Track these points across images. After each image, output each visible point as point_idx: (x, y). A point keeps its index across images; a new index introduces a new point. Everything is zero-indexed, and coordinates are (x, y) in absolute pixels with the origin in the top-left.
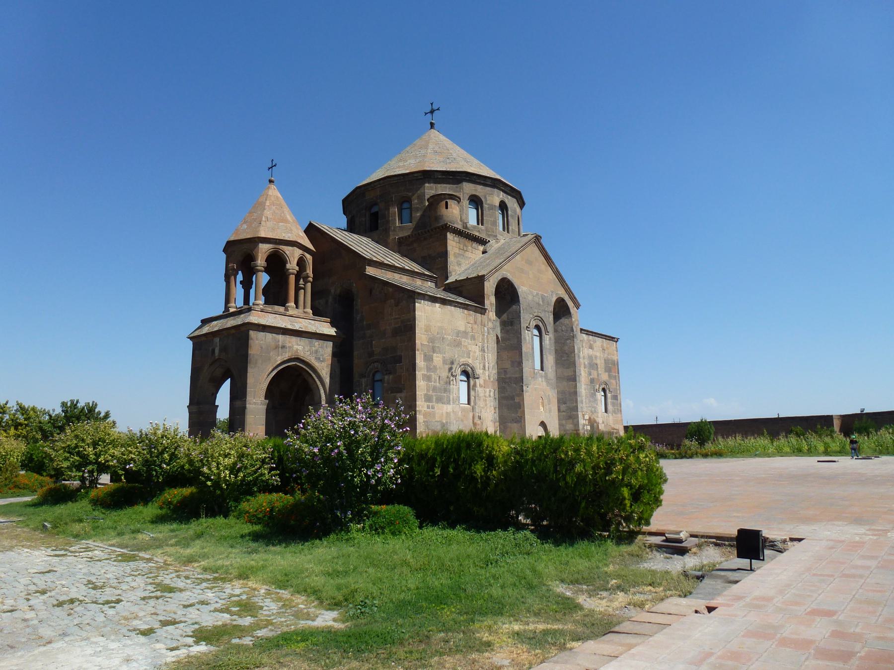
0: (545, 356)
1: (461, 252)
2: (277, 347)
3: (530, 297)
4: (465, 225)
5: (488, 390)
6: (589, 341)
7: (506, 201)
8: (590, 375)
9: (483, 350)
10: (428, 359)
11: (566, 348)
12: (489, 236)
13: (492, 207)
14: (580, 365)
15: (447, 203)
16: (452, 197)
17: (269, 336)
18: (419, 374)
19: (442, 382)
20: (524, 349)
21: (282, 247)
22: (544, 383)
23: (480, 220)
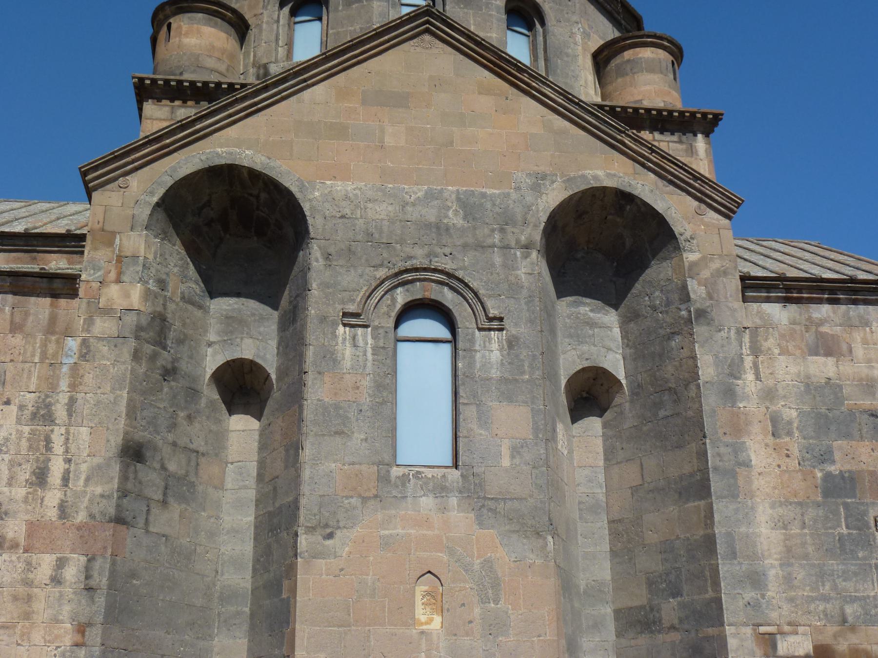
0: (468, 412)
3: (382, 211)
5: (46, 563)
6: (811, 323)
8: (825, 457)
9: (43, 415)
11: (669, 369)
14: (738, 426)
15: (169, 26)
20: (318, 392)
22: (459, 518)
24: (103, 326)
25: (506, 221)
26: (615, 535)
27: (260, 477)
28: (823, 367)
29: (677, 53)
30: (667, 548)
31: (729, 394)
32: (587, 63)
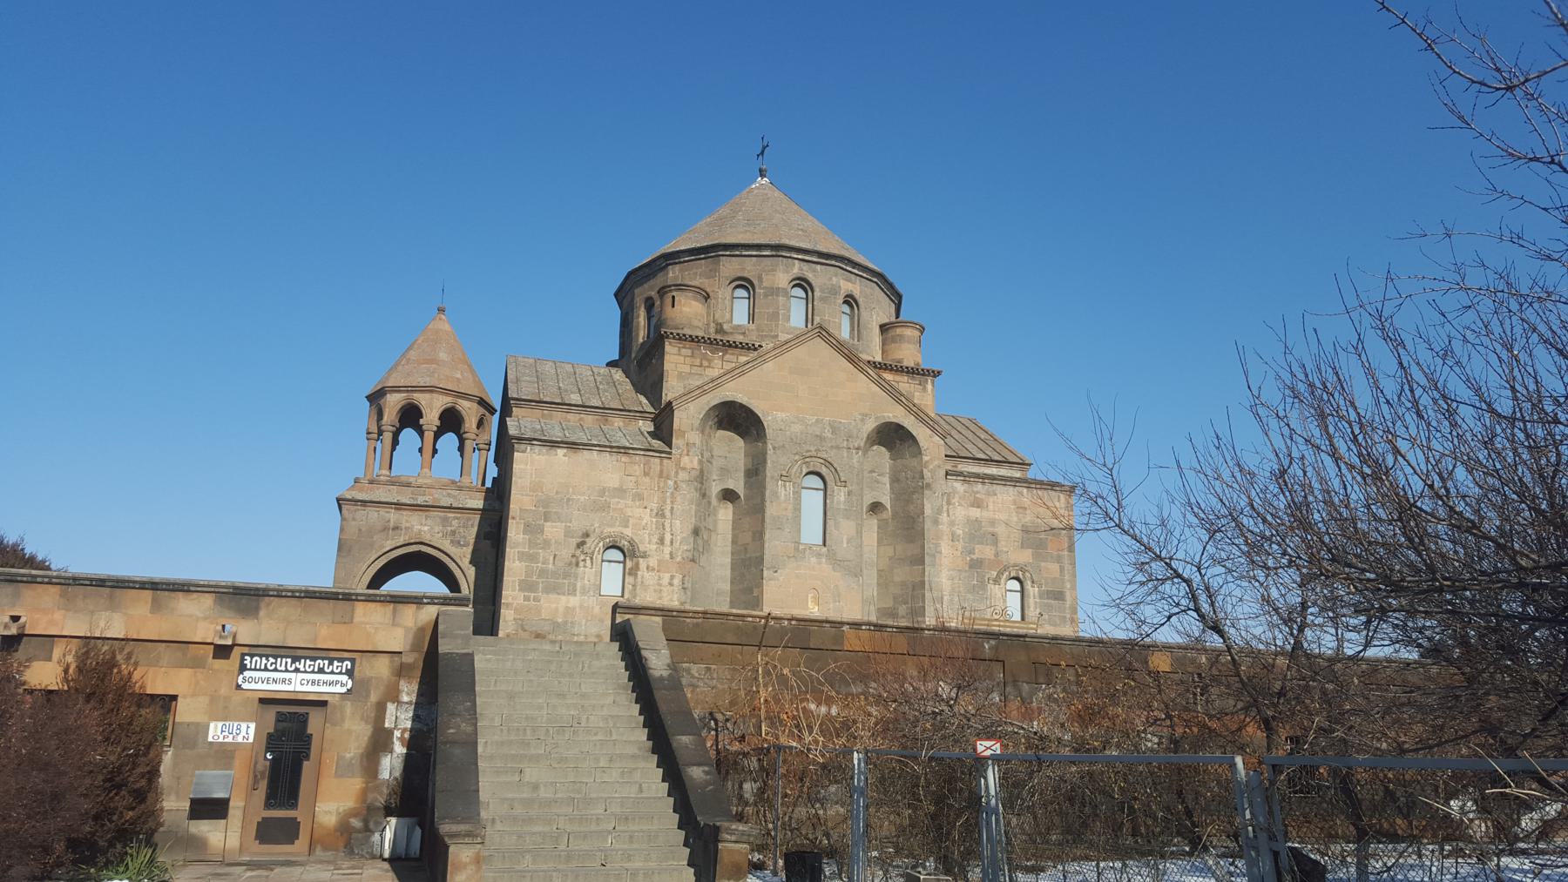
0: (830, 523)
1: (695, 370)
2: (385, 529)
3: (797, 428)
4: (720, 330)
5: (666, 577)
7: (810, 276)
8: (971, 552)
9: (660, 514)
10: (532, 529)
12: (763, 337)
13: (774, 292)
16: (681, 287)
17: (373, 514)
18: (511, 553)
19: (560, 564)
20: (771, 510)
21: (416, 395)
22: (826, 568)
23: (752, 317)
24: (683, 475)
25: (849, 437)
26: (880, 576)
27: (734, 542)
28: (975, 513)
29: (922, 330)
30: (903, 584)
31: (936, 522)
32: (877, 330)
